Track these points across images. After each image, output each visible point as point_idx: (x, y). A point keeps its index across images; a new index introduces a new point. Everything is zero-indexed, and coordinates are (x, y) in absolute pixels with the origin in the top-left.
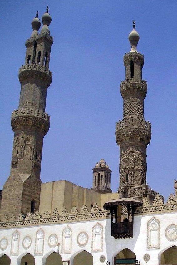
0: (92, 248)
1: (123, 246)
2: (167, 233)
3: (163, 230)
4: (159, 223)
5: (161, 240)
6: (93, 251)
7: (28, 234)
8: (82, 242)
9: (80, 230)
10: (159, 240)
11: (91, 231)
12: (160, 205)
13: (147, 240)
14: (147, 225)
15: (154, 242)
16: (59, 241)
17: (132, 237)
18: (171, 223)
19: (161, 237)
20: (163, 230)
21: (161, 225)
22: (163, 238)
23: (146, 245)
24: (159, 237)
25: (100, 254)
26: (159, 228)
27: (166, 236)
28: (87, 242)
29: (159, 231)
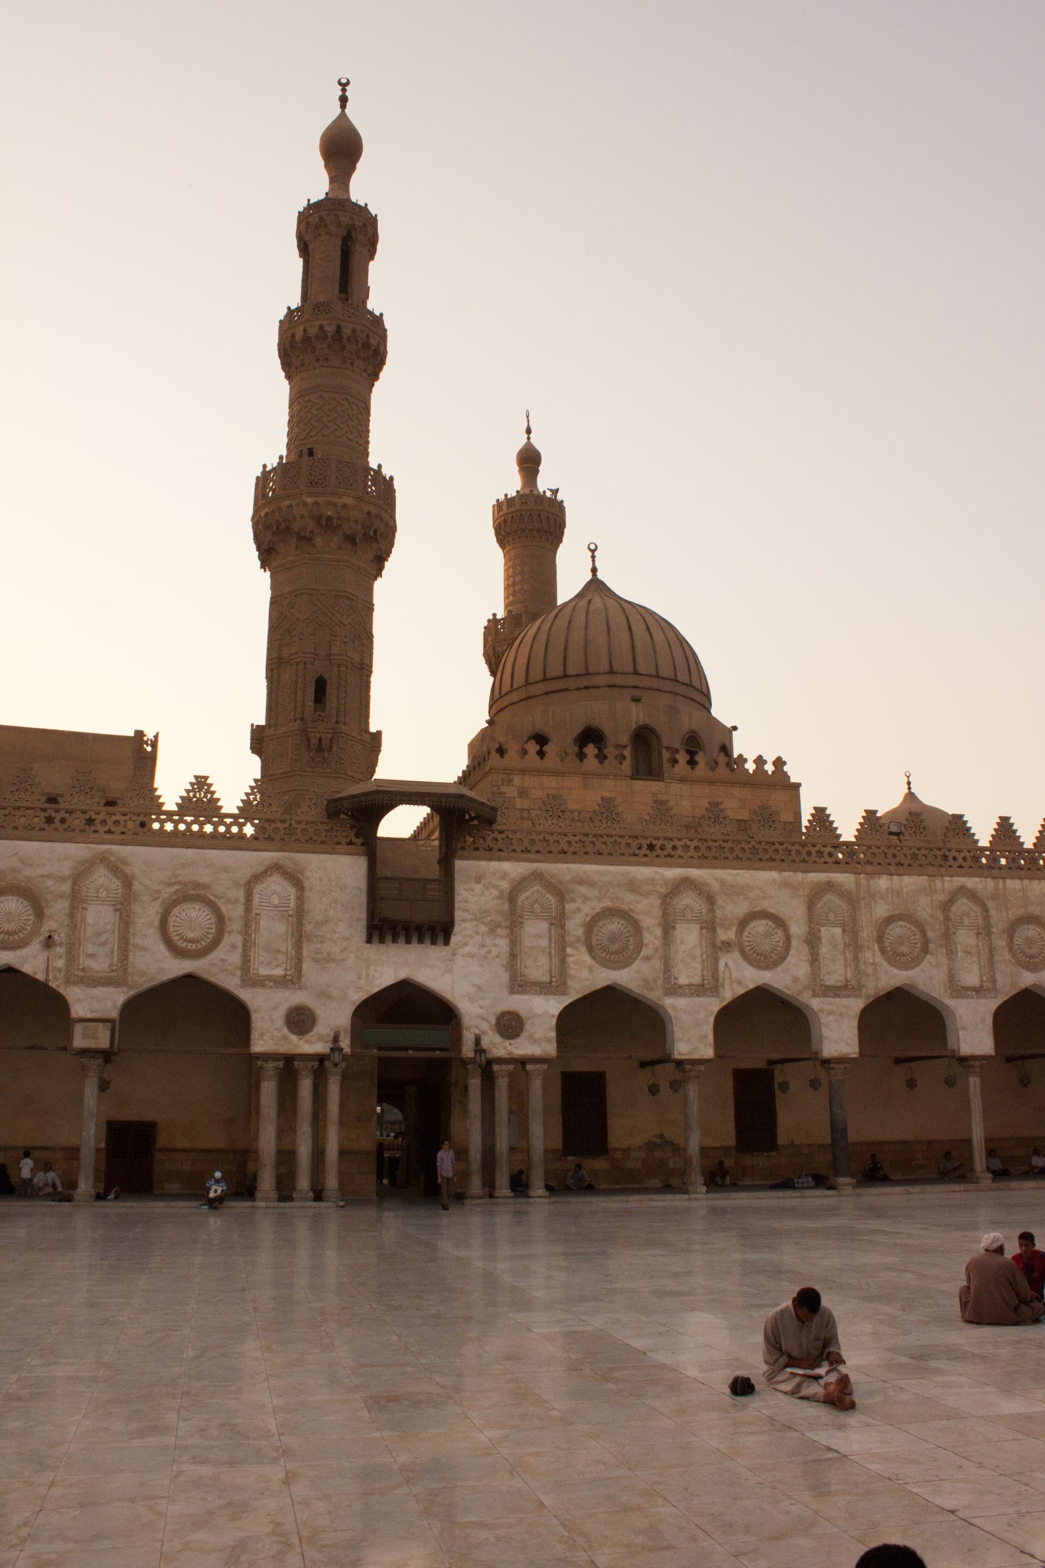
1: (402, 976)
2: (594, 943)
3: (575, 926)
5: (570, 960)
6: (251, 981)
9: (177, 887)
10: (563, 961)
11: (240, 895)
13: (513, 955)
14: (512, 897)
17: (447, 942)
18: (610, 904)
19: (569, 950)
20: (575, 926)
21: (569, 907)
22: (579, 959)
23: (506, 977)
24: (562, 950)
27: (590, 949)
29: (563, 927)
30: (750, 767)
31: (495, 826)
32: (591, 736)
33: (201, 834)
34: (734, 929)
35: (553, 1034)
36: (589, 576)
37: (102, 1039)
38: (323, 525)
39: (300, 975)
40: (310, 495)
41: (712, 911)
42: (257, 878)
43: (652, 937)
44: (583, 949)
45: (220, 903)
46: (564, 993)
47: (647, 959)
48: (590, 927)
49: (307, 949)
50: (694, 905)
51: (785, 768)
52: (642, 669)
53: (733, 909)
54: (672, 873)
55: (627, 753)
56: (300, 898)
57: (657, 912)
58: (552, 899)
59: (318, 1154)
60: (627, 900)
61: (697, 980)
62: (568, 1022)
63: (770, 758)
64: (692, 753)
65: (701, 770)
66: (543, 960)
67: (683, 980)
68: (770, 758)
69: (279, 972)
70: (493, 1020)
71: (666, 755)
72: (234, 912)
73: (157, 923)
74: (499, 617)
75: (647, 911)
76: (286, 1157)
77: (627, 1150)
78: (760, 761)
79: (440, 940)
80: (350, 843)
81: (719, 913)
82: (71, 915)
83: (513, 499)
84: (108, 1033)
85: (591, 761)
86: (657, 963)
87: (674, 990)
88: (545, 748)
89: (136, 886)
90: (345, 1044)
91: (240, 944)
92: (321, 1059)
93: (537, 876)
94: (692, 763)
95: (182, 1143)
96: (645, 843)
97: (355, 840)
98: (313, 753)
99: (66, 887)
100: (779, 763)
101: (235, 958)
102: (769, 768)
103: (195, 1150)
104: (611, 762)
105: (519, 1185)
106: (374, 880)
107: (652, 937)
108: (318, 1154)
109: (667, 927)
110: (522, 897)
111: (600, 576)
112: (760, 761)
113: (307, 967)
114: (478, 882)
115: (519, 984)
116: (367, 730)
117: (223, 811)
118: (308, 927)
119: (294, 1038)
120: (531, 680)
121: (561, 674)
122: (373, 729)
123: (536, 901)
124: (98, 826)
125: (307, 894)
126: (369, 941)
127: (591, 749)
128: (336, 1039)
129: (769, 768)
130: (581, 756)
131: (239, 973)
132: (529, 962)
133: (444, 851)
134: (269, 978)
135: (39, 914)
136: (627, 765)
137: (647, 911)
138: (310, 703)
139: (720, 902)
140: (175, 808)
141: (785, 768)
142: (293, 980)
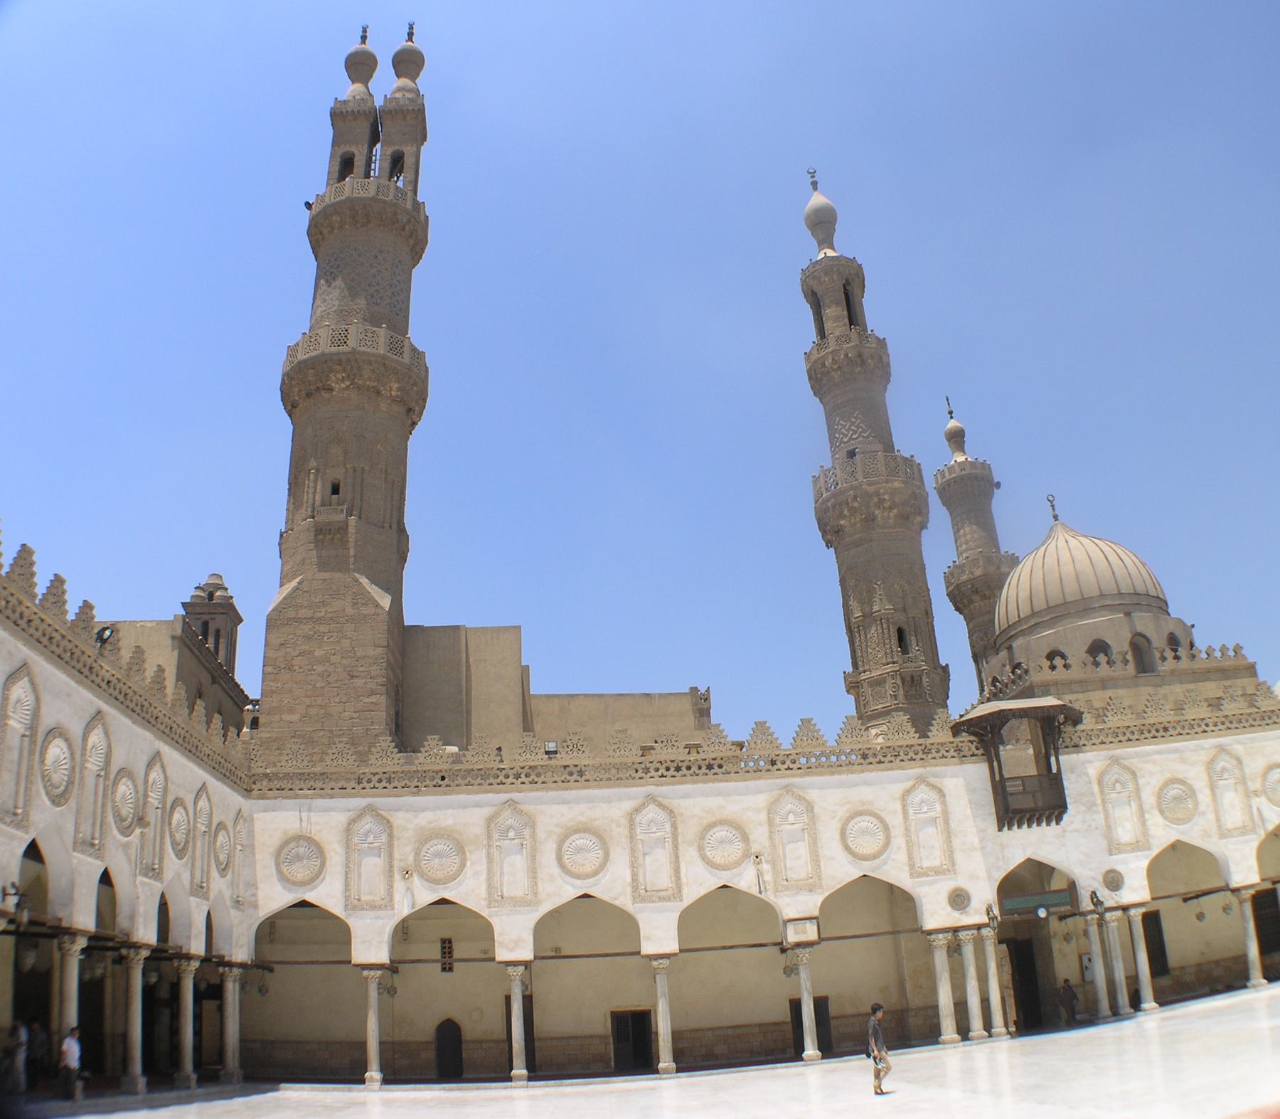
0: (912, 866)
3: (1149, 798)
4: (1134, 774)
5: (1149, 823)
7: (583, 819)
8: (868, 845)
9: (848, 806)
11: (898, 807)
15: (1126, 831)
16: (755, 848)
18: (1168, 775)
19: (1147, 816)
20: (1149, 798)
21: (1141, 781)
22: (1155, 821)
25: (945, 886)
26: (1138, 790)
27: (1162, 812)
28: (886, 845)
29: (1139, 798)
31: (1080, 727)
32: (1098, 648)
34: (1259, 780)
35: (1146, 882)
37: (811, 933)
39: (953, 864)
40: (870, 484)
41: (1242, 769)
42: (908, 792)
43: (1204, 796)
44: (1156, 813)
45: (883, 815)
46: (1149, 849)
47: (1204, 813)
48: (1160, 795)
49: (956, 843)
50: (1228, 766)
51: (1243, 652)
53: (1254, 765)
54: (1209, 742)
55: (1129, 657)
56: (944, 803)
57: (1205, 777)
58: (1127, 777)
59: (985, 1002)
60: (1182, 771)
61: (1240, 824)
62: (1155, 870)
63: (1231, 646)
64: (1175, 651)
66: (1128, 825)
67: (1230, 826)
69: (936, 863)
70: (1101, 879)
71: (1157, 655)
72: (895, 821)
73: (837, 836)
75: (1197, 777)
76: (961, 1008)
77: (1182, 968)
79: (1054, 823)
80: (973, 755)
81: (1247, 770)
82: (771, 838)
83: (952, 467)
84: (815, 928)
86: (1211, 816)
87: (1224, 834)
89: (817, 810)
90: (996, 911)
91: (904, 846)
92: (979, 927)
94: (1177, 658)
95: (850, 1010)
96: (1160, 727)
97: (977, 752)
99: (763, 817)
100: (1237, 649)
101: (902, 857)
103: (859, 1015)
104: (1119, 665)
105: (1136, 1002)
107: (1204, 796)
108: (985, 1002)
109: (1213, 788)
110: (1106, 778)
112: (1224, 649)
113: (958, 857)
114: (1073, 772)
115: (1114, 847)
118: (953, 825)
119: (956, 914)
123: (1117, 781)
125: (948, 798)
126: (1000, 830)
127: (1102, 658)
128: (989, 910)
130: (1097, 664)
131: (907, 868)
132: (1120, 831)
134: (930, 869)
135: (745, 838)
136: (1131, 668)
137: (1197, 777)
139: (1245, 761)
141: (1243, 652)
142: (949, 868)
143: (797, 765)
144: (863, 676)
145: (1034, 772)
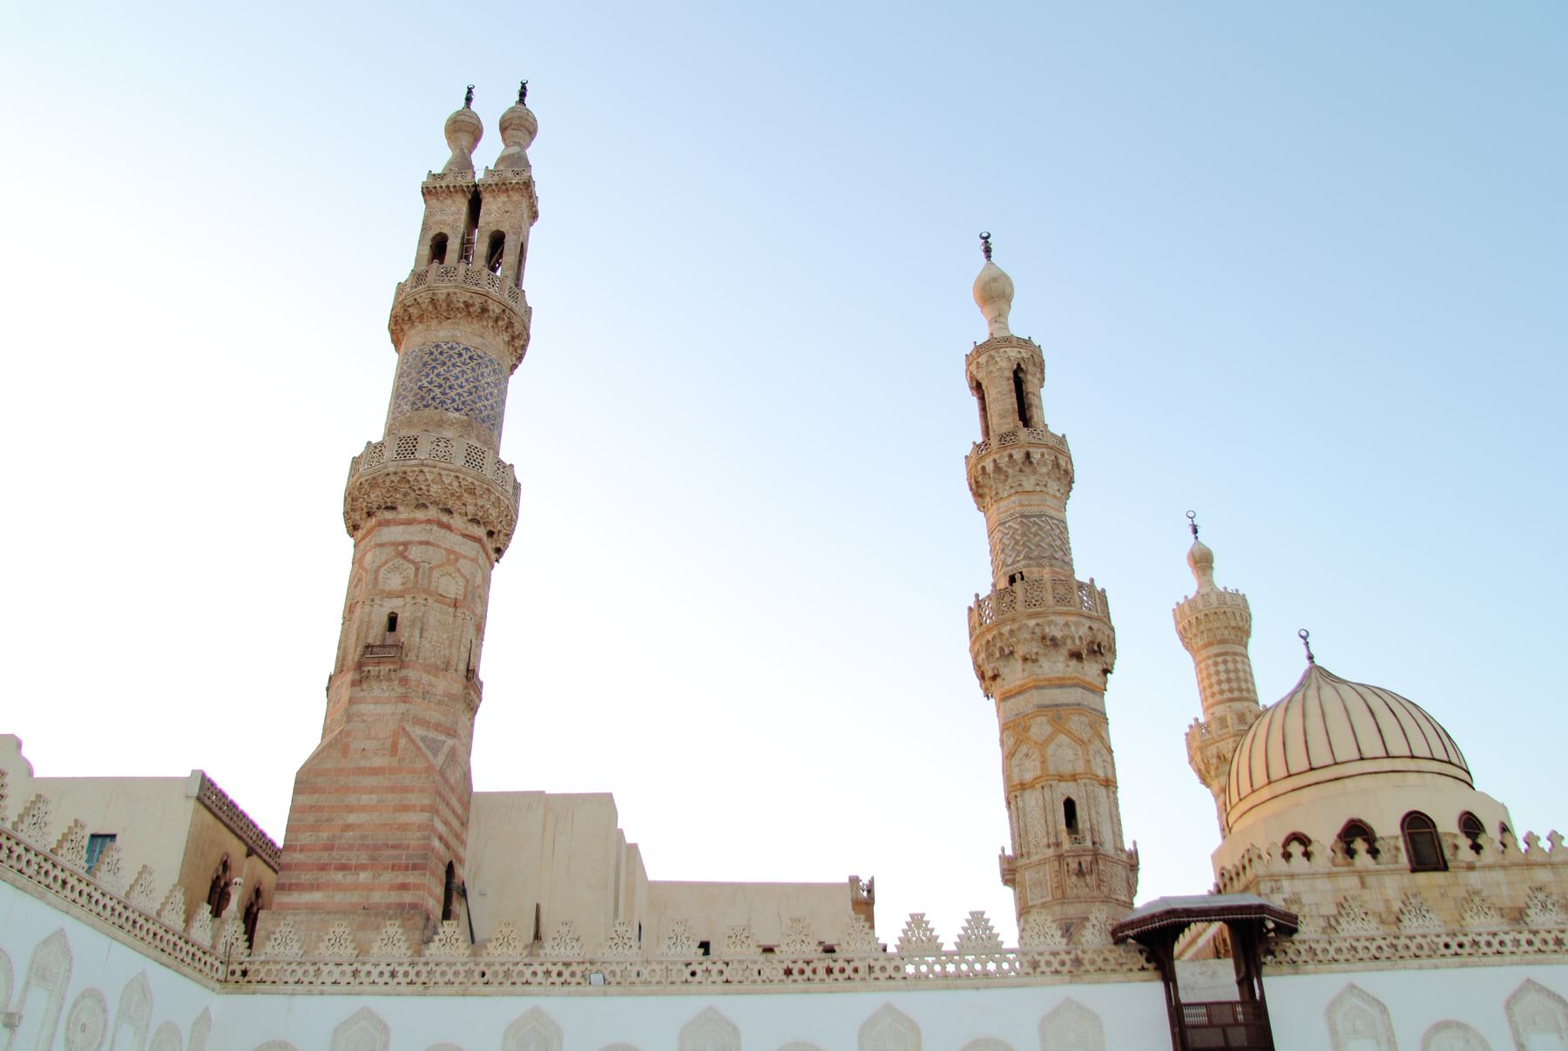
12: (1371, 933)
30: (1523, 846)
32: (1355, 832)
33: (945, 975)
36: (1306, 664)
38: (1040, 639)
52: (1393, 752)
65: (1488, 855)
68: (1542, 834)
74: (1202, 720)
78: (1531, 840)
85: (1363, 859)
88: (1310, 849)
93: (1352, 987)
98: (1074, 878)
102: (1545, 845)
106: (1176, 1010)
111: (1317, 661)
116: (1123, 850)
117: (1005, 946)
120: (1273, 777)
121: (1307, 767)
122: (1128, 846)
124: (877, 973)
129: (1545, 845)
133: (1243, 969)
138: (1063, 826)
140: (954, 948)
143: (898, 975)
144: (1025, 861)
145: (1237, 998)
